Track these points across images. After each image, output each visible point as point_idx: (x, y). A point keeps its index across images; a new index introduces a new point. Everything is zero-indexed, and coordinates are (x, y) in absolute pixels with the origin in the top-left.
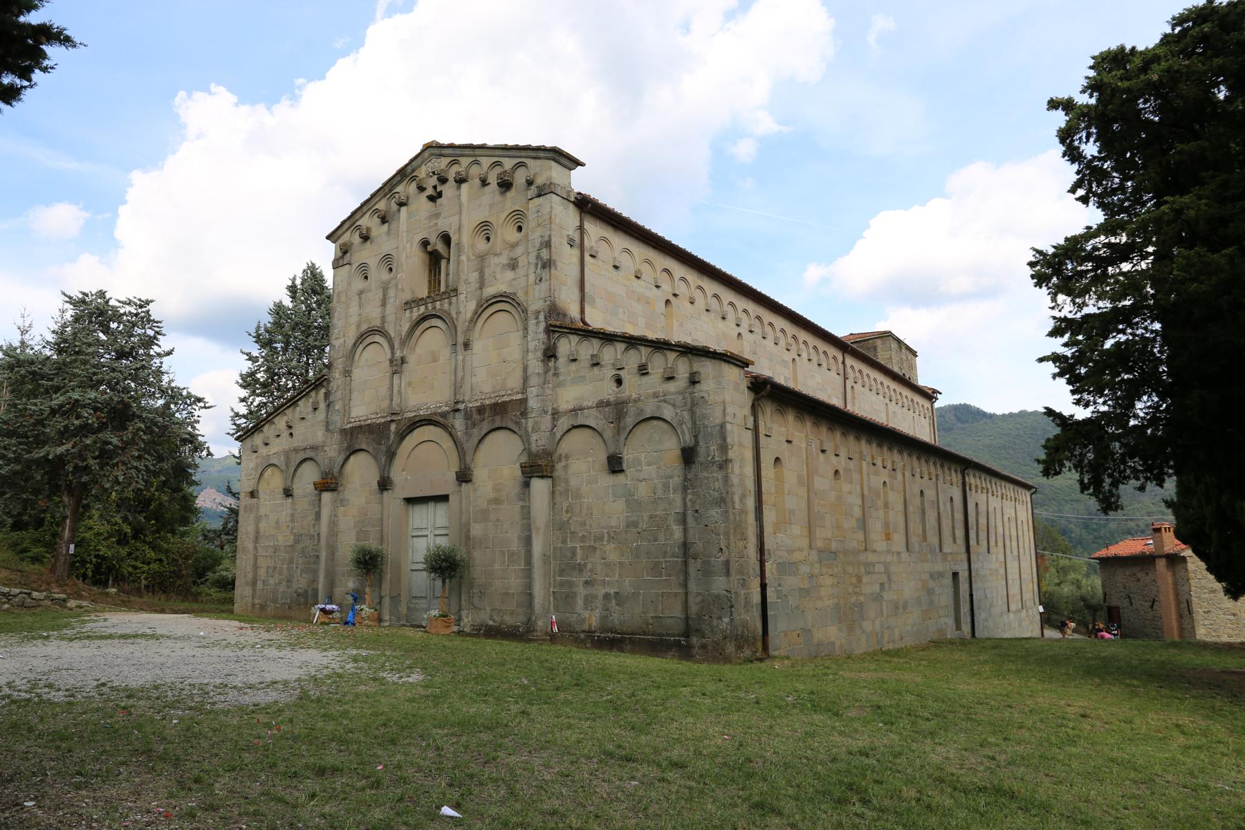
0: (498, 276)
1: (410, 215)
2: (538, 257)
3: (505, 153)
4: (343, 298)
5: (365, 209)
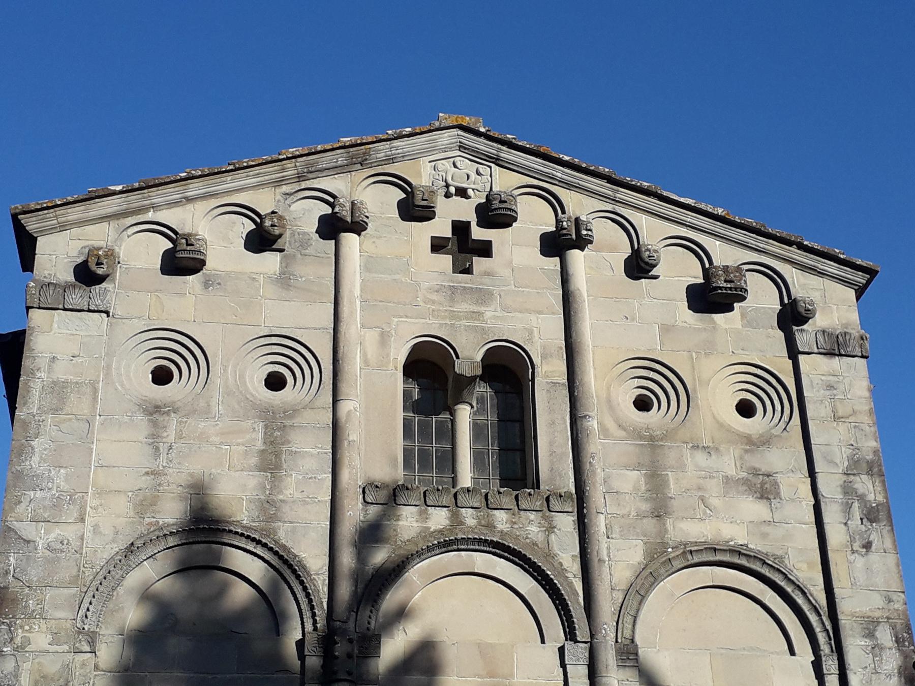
0: (715, 502)
1: (369, 264)
2: (848, 490)
3: (718, 227)
4: (78, 404)
5: (195, 188)
